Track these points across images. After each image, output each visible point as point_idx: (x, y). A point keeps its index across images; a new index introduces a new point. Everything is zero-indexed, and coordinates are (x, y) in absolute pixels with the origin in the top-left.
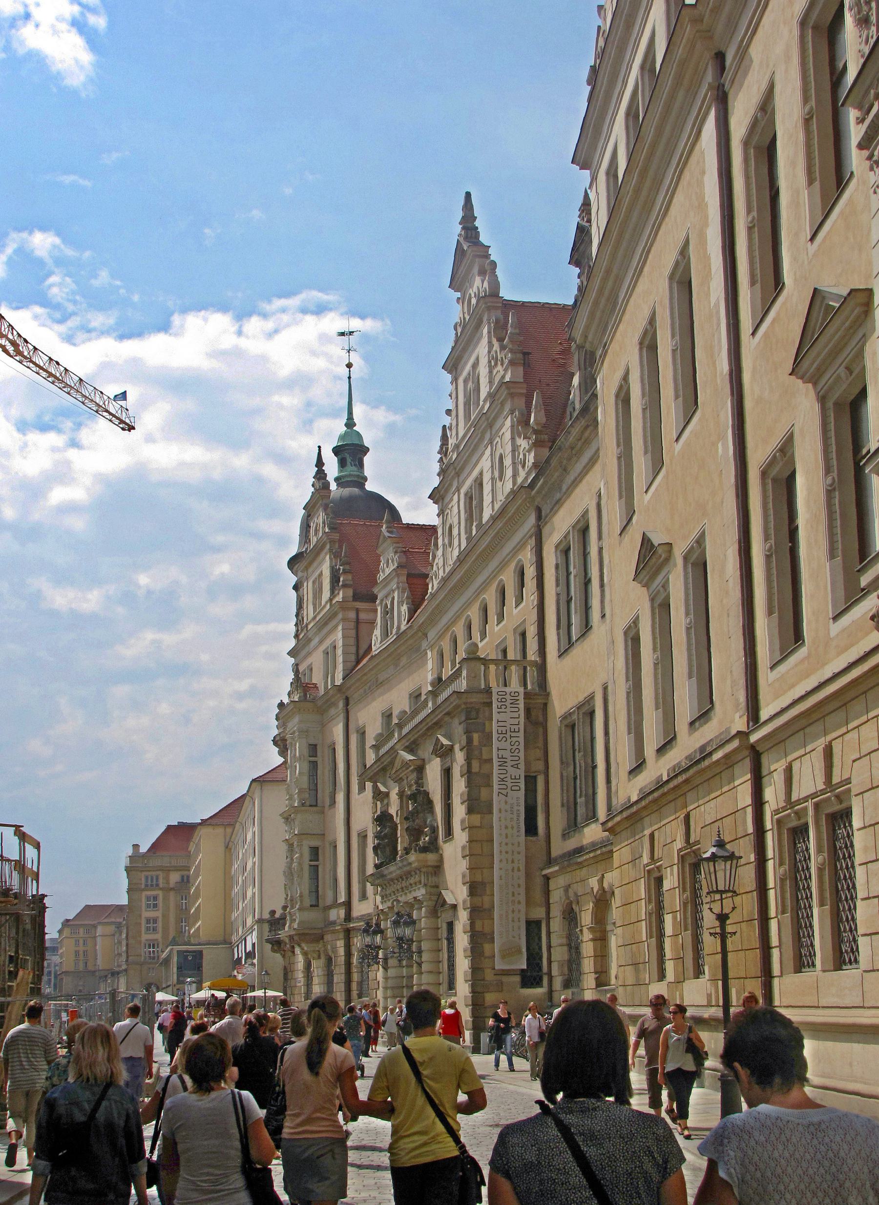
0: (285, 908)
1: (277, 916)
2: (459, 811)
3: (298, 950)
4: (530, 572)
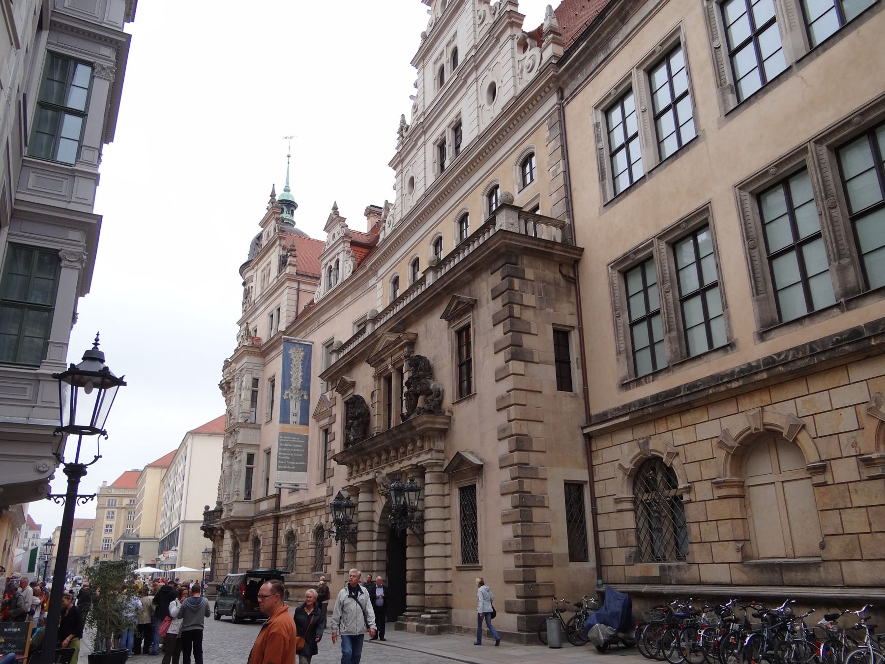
0: (219, 503)
1: (212, 509)
3: (227, 535)
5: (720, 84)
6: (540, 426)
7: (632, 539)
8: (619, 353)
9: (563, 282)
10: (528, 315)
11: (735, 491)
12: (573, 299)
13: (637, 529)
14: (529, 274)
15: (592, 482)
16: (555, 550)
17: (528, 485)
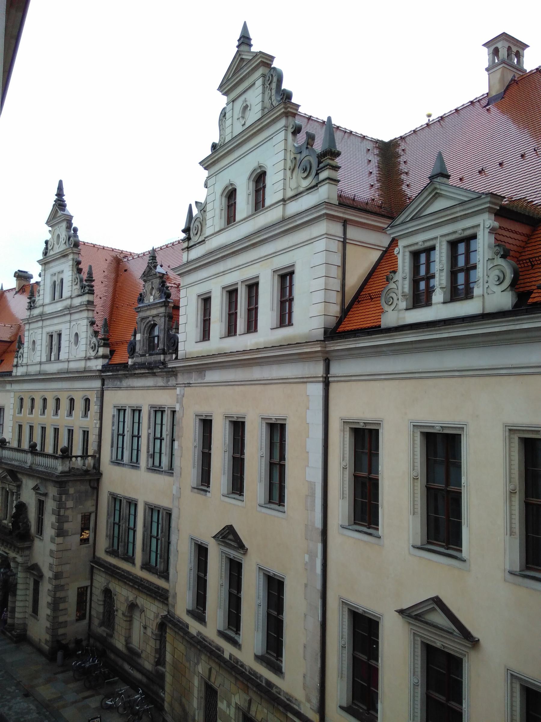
2: (49, 531)
4: (94, 408)
5: (148, 452)
6: (68, 566)
7: (101, 617)
8: (107, 536)
9: (90, 489)
10: (69, 513)
11: (128, 619)
12: (95, 498)
13: (104, 613)
14: (71, 491)
15: (91, 585)
16: (68, 619)
17: (58, 595)
